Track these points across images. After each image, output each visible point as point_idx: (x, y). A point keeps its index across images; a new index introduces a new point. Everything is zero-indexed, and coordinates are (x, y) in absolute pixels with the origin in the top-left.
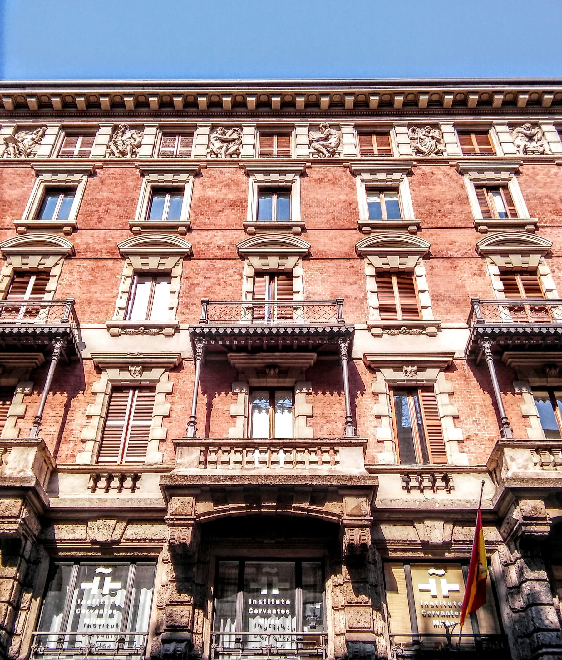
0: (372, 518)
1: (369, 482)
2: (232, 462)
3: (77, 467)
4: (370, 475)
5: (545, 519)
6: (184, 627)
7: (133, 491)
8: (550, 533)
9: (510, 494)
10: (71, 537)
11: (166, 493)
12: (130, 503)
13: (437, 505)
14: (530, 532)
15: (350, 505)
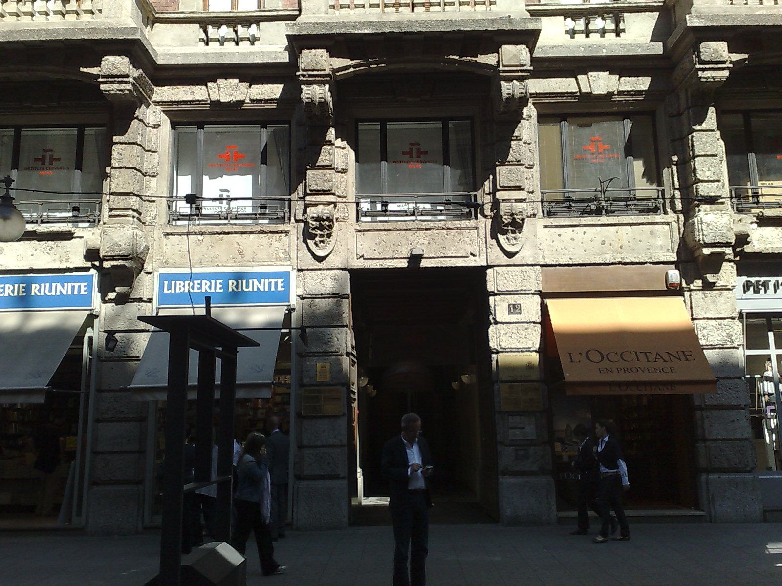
0: (532, 68)
1: (531, 26)
2: (457, 4)
3: (182, 15)
4: (532, 17)
5: (724, 62)
6: (329, 191)
7: (618, 35)
8: (728, 78)
9: (691, 35)
10: (189, 98)
11: (294, 45)
12: (252, 57)
13: (604, 51)
14: (706, 78)
15: (514, 54)
